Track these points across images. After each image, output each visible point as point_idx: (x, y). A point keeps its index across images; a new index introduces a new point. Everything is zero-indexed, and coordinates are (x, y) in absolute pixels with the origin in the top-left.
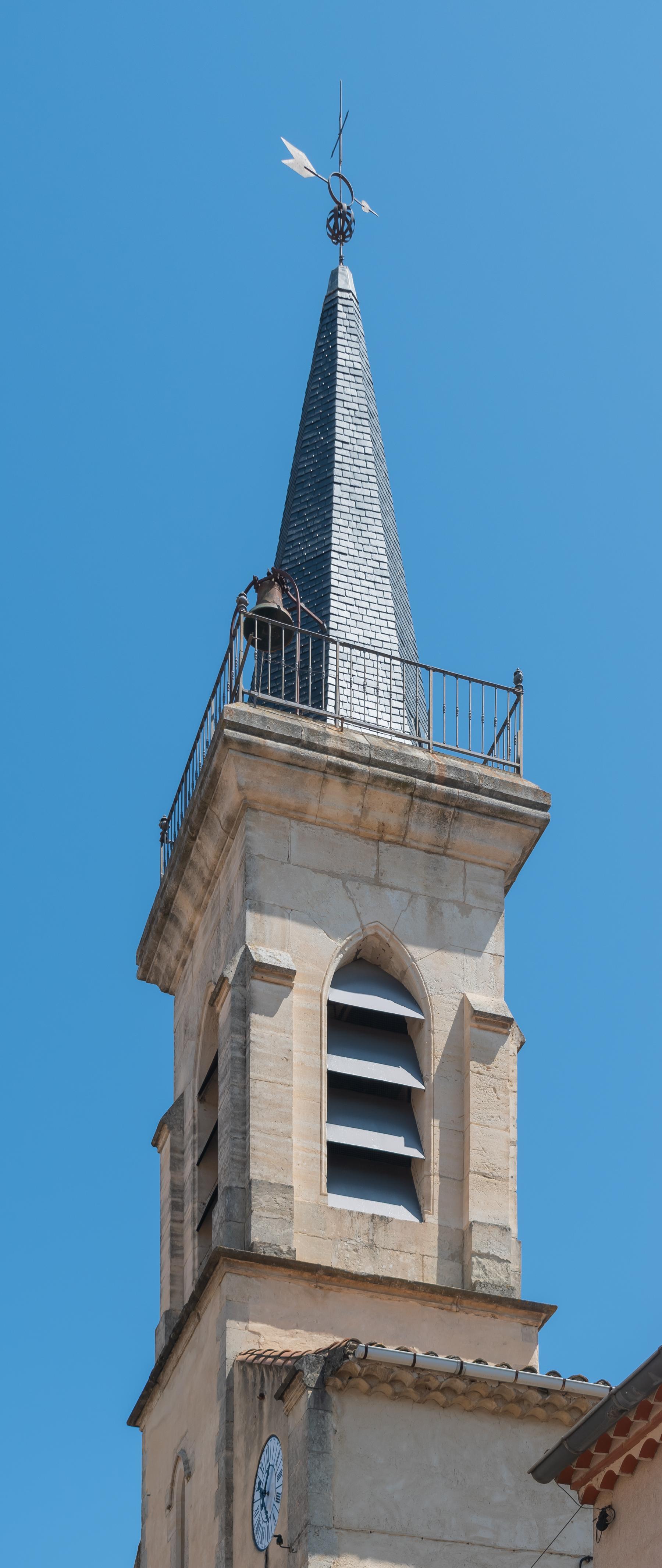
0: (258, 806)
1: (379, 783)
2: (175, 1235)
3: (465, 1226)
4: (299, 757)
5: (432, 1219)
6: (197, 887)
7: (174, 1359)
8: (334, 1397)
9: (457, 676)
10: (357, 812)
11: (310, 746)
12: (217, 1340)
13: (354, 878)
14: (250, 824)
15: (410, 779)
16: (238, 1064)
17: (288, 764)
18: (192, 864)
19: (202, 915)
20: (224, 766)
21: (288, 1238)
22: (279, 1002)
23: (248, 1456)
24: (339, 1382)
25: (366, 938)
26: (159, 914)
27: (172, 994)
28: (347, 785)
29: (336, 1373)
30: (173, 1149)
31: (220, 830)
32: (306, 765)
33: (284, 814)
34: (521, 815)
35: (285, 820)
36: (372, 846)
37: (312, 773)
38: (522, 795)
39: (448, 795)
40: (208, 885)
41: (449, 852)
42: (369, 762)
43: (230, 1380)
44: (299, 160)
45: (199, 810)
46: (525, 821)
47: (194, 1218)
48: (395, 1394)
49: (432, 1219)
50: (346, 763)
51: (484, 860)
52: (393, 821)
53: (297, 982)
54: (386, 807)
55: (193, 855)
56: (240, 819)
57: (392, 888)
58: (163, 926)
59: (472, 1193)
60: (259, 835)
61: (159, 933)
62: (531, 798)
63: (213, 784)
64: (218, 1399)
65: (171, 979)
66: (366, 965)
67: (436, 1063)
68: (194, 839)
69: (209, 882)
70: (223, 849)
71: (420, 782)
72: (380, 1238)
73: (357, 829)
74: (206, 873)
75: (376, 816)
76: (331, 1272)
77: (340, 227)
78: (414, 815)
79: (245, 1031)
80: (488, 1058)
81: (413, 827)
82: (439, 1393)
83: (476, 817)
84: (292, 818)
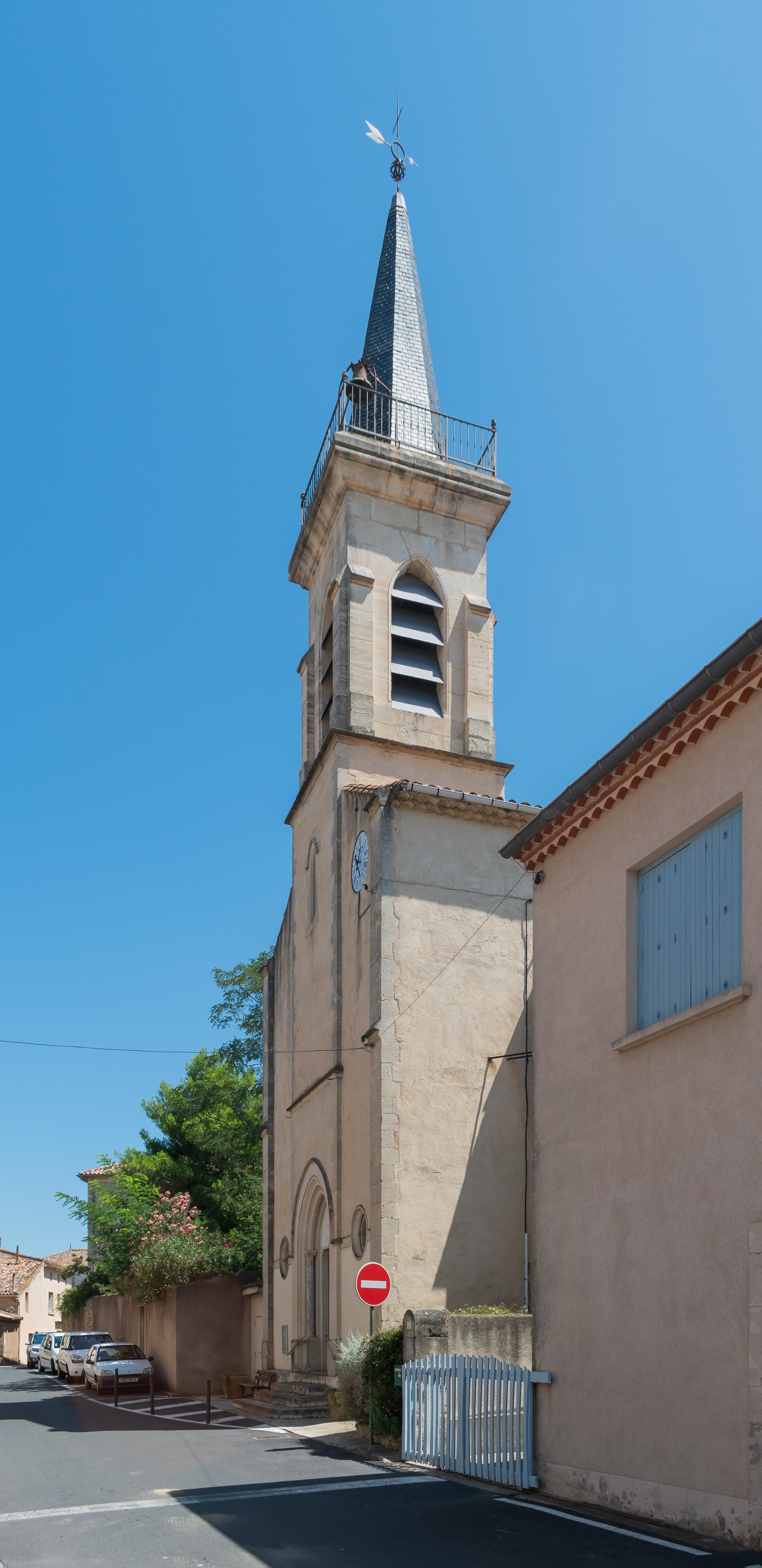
0: (354, 488)
4: (376, 462)
8: (395, 811)
11: (382, 456)
13: (406, 529)
16: (343, 629)
17: (370, 466)
21: (371, 724)
22: (366, 596)
24: (398, 803)
28: (402, 478)
30: (308, 675)
32: (379, 467)
34: (496, 498)
35: (368, 496)
36: (415, 512)
37: (383, 472)
39: (456, 486)
42: (413, 466)
44: (375, 134)
46: (497, 502)
48: (428, 810)
50: (401, 466)
52: (427, 499)
53: (375, 585)
54: (423, 492)
57: (426, 535)
60: (354, 504)
62: (500, 489)
63: (330, 476)
66: (412, 577)
67: (450, 632)
71: (441, 478)
73: (407, 503)
77: (398, 172)
79: (347, 611)
81: (437, 503)
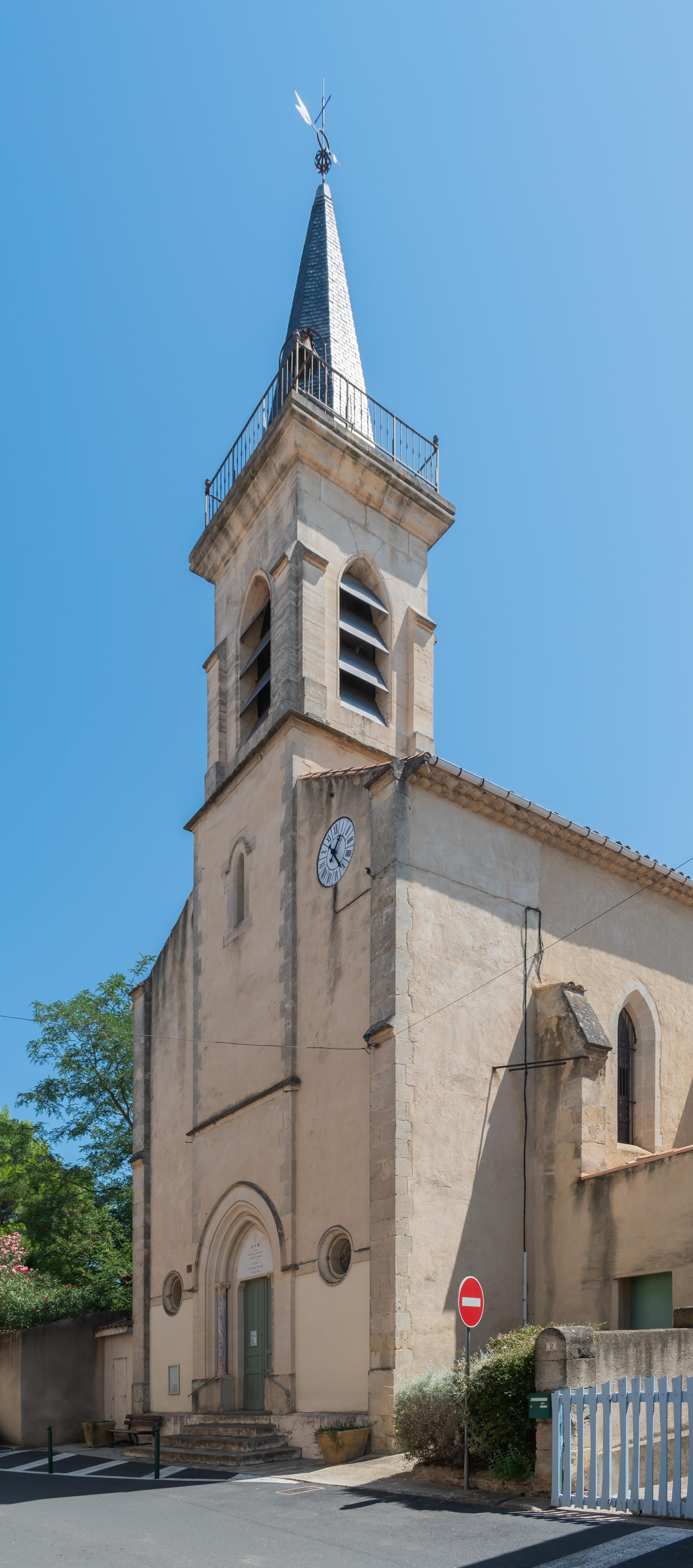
0: (305, 461)
1: (372, 468)
2: (222, 720)
3: (410, 734)
4: (332, 437)
5: (393, 726)
6: (248, 511)
7: (233, 784)
8: (410, 788)
9: (407, 426)
10: (358, 483)
11: (337, 432)
12: (282, 768)
13: (354, 521)
14: (299, 470)
15: (388, 472)
16: (293, 609)
17: (325, 439)
18: (248, 496)
19: (247, 531)
20: (287, 430)
21: (324, 715)
22: (318, 578)
23: (313, 832)
24: (415, 778)
25: (357, 560)
26: (216, 528)
27: (213, 583)
28: (355, 464)
29: (415, 771)
30: (220, 669)
31: (275, 473)
32: (334, 444)
33: (318, 471)
34: (441, 513)
35: (317, 474)
36: (362, 507)
37: (337, 450)
38: (442, 502)
39: (407, 489)
40: (257, 511)
41: (402, 524)
42: (368, 454)
43: (294, 791)
44: (303, 109)
45: (262, 458)
46: (442, 516)
47: (237, 710)
48: (443, 792)
49: (393, 726)
50: (356, 450)
51: (418, 535)
52: (376, 495)
53: (328, 567)
54: (374, 485)
55: (250, 490)
56: (291, 467)
57: (373, 534)
58: (216, 536)
59: (415, 716)
60: (305, 479)
61: (212, 541)
62: (446, 505)
63: (276, 441)
64: (283, 802)
65: (215, 573)
66: (353, 575)
67: (395, 640)
68: (253, 478)
69: (258, 509)
70: (274, 487)
71: (393, 476)
72: (367, 729)
73: (356, 493)
74: (257, 502)
75: (368, 489)
76: (350, 740)
77: (323, 162)
78: (387, 496)
79: (299, 590)
80: (423, 644)
81: (386, 502)
82: (464, 797)
83: (418, 507)
84: (321, 475)
